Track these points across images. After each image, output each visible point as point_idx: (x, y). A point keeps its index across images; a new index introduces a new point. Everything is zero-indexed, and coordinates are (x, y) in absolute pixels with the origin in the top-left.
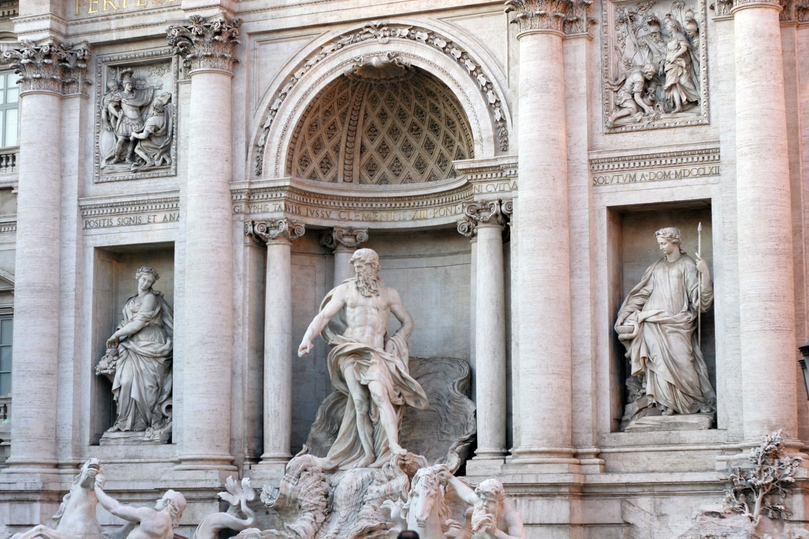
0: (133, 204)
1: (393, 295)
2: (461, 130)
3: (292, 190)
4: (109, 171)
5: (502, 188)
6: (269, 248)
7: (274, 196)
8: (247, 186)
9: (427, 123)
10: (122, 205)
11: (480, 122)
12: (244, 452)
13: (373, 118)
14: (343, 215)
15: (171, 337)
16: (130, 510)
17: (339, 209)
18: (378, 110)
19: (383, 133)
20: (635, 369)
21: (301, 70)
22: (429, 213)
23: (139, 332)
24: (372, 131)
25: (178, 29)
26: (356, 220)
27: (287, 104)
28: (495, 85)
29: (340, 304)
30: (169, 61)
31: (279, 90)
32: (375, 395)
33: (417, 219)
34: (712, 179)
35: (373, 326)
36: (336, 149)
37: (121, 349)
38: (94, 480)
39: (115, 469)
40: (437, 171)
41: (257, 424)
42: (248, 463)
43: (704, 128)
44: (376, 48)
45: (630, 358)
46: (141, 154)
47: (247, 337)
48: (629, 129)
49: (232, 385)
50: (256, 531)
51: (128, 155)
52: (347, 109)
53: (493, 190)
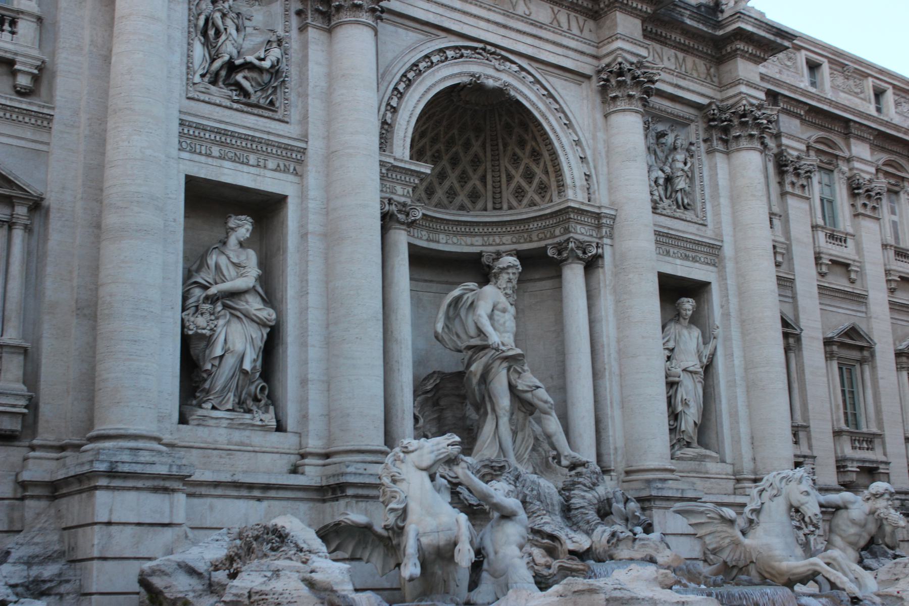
0: (246, 138)
4: (203, 90)
7: (407, 179)
8: (392, 161)
10: (233, 135)
11: (572, 170)
18: (423, 128)
19: (415, 150)
20: (680, 408)
22: (442, 237)
27: (414, 90)
28: (584, 143)
31: (404, 75)
32: (546, 402)
37: (219, 307)
39: (221, 457)
40: (446, 201)
43: (703, 228)
44: (491, 72)
46: (246, 84)
48: (664, 212)
51: (221, 80)
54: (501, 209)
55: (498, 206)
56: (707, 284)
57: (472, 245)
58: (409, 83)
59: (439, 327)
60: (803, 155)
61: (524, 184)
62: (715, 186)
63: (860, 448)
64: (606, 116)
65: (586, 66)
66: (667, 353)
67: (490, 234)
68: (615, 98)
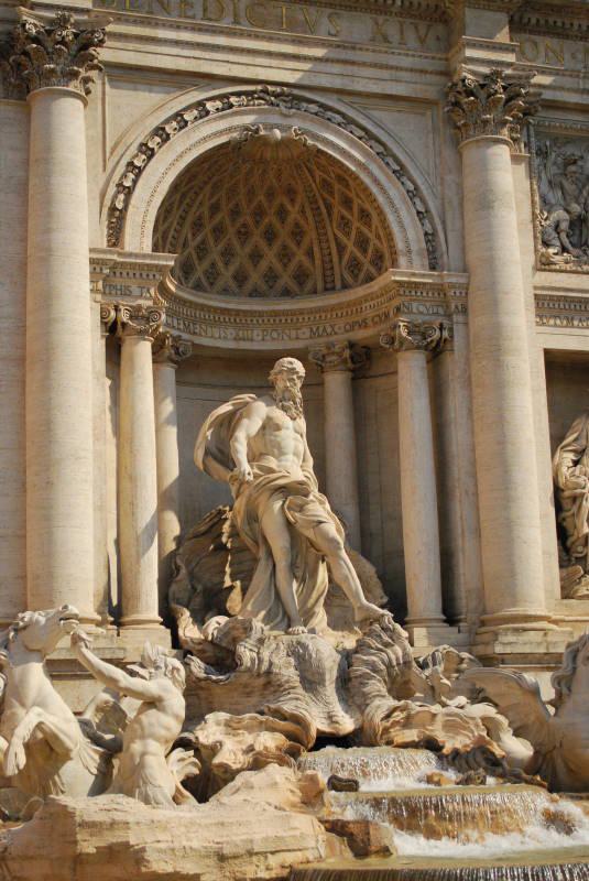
2: (316, 242)
5: (435, 311)
8: (115, 257)
9: (262, 227)
11: (406, 230)
18: (214, 200)
19: (208, 228)
21: (174, 124)
22: (257, 334)
24: (198, 225)
25: (35, 26)
26: (178, 329)
29: (260, 423)
33: (240, 339)
35: (295, 454)
36: (164, 237)
42: (115, 627)
48: (563, 268)
50: (223, 716)
52: (192, 188)
53: (425, 312)
54: (333, 289)
55: (329, 286)
57: (297, 338)
58: (151, 154)
59: (199, 454)
61: (359, 255)
64: (461, 156)
65: (427, 88)
66: (571, 456)
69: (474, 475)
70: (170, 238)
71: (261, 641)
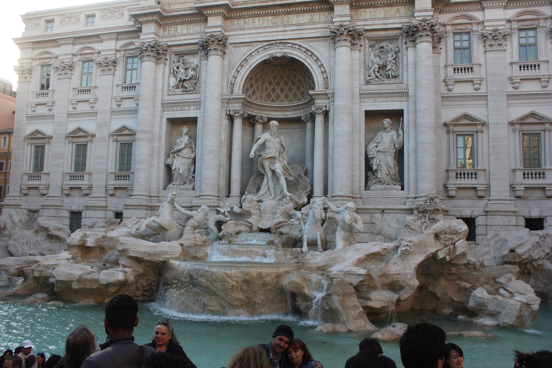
0: (182, 103)
1: (282, 138)
3: (245, 99)
6: (235, 120)
10: (178, 103)
12: (224, 192)
13: (271, 78)
14: (259, 112)
15: (195, 152)
16: (189, 212)
17: (258, 109)
18: (274, 75)
19: (274, 83)
23: (182, 149)
24: (270, 83)
30: (197, 53)
31: (241, 64)
34: (404, 103)
36: (258, 88)
37: (176, 155)
38: (174, 200)
40: (293, 98)
41: (227, 184)
44: (279, 50)
45: (372, 164)
46: (186, 85)
47: (225, 152)
49: (219, 170)
50: (233, 222)
56: (403, 110)
60: (500, 28)
62: (407, 65)
63: (532, 178)
65: (327, 33)
67: (304, 108)
68: (334, 43)
69: (333, 152)
70: (260, 88)
71: (250, 202)
